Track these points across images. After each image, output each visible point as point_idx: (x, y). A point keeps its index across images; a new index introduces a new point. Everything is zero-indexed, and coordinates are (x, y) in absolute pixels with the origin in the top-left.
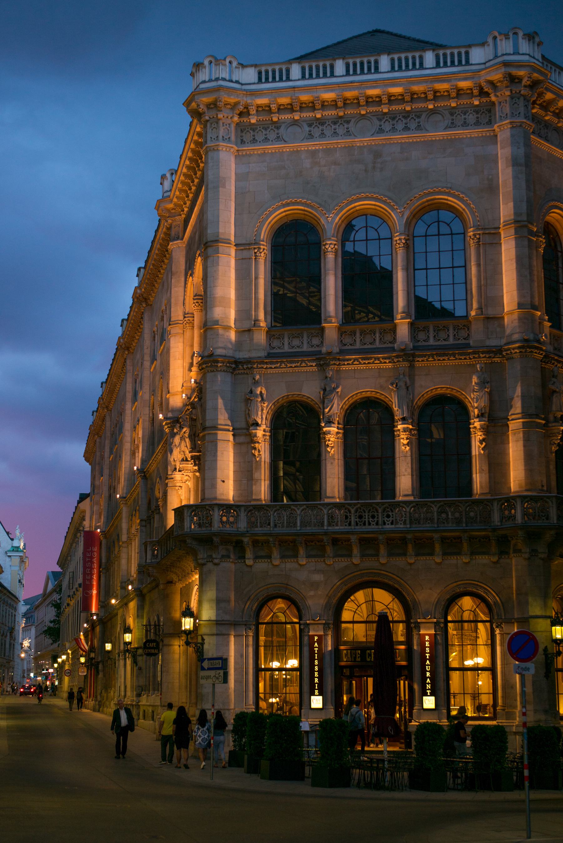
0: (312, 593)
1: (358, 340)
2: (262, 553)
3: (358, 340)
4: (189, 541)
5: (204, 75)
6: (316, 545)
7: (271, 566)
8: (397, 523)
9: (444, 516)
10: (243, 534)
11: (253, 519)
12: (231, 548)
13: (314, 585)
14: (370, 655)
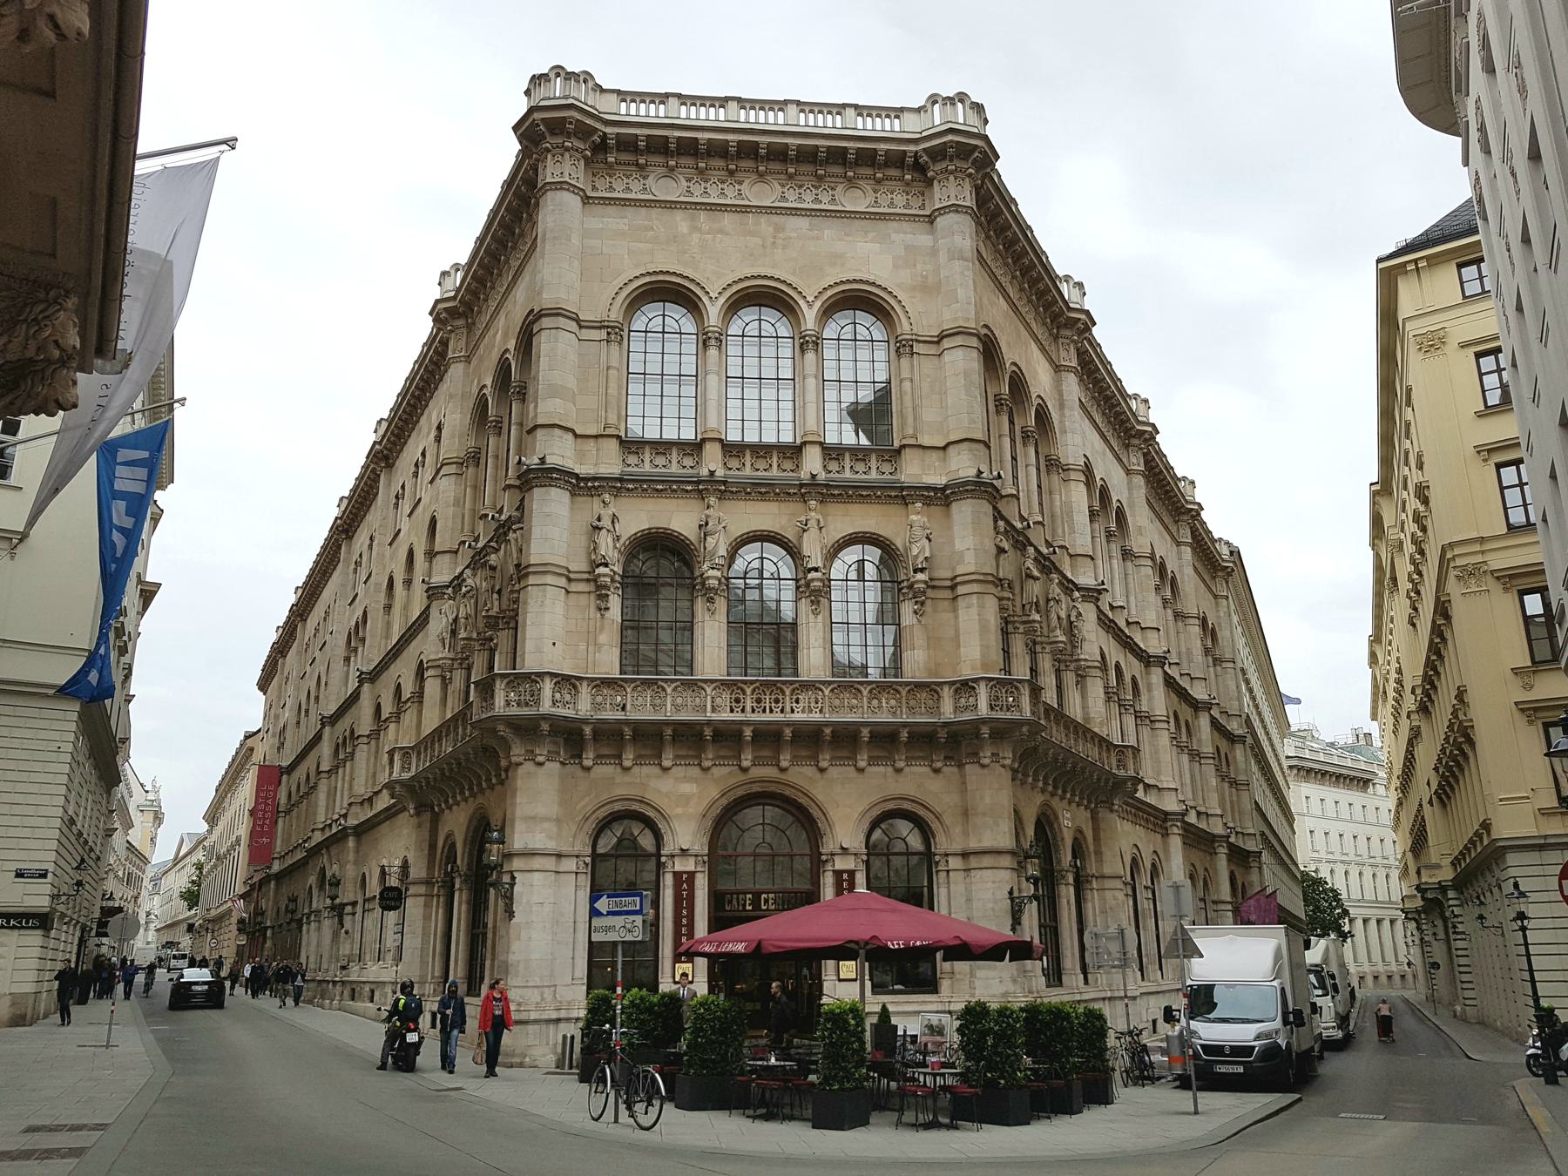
0: (679, 811)
1: (748, 464)
2: (606, 751)
3: (748, 464)
4: (501, 727)
5: (541, 92)
6: (691, 739)
7: (619, 769)
8: (811, 711)
9: (875, 702)
10: (585, 721)
11: (599, 699)
12: (561, 741)
13: (686, 799)
14: (766, 901)
